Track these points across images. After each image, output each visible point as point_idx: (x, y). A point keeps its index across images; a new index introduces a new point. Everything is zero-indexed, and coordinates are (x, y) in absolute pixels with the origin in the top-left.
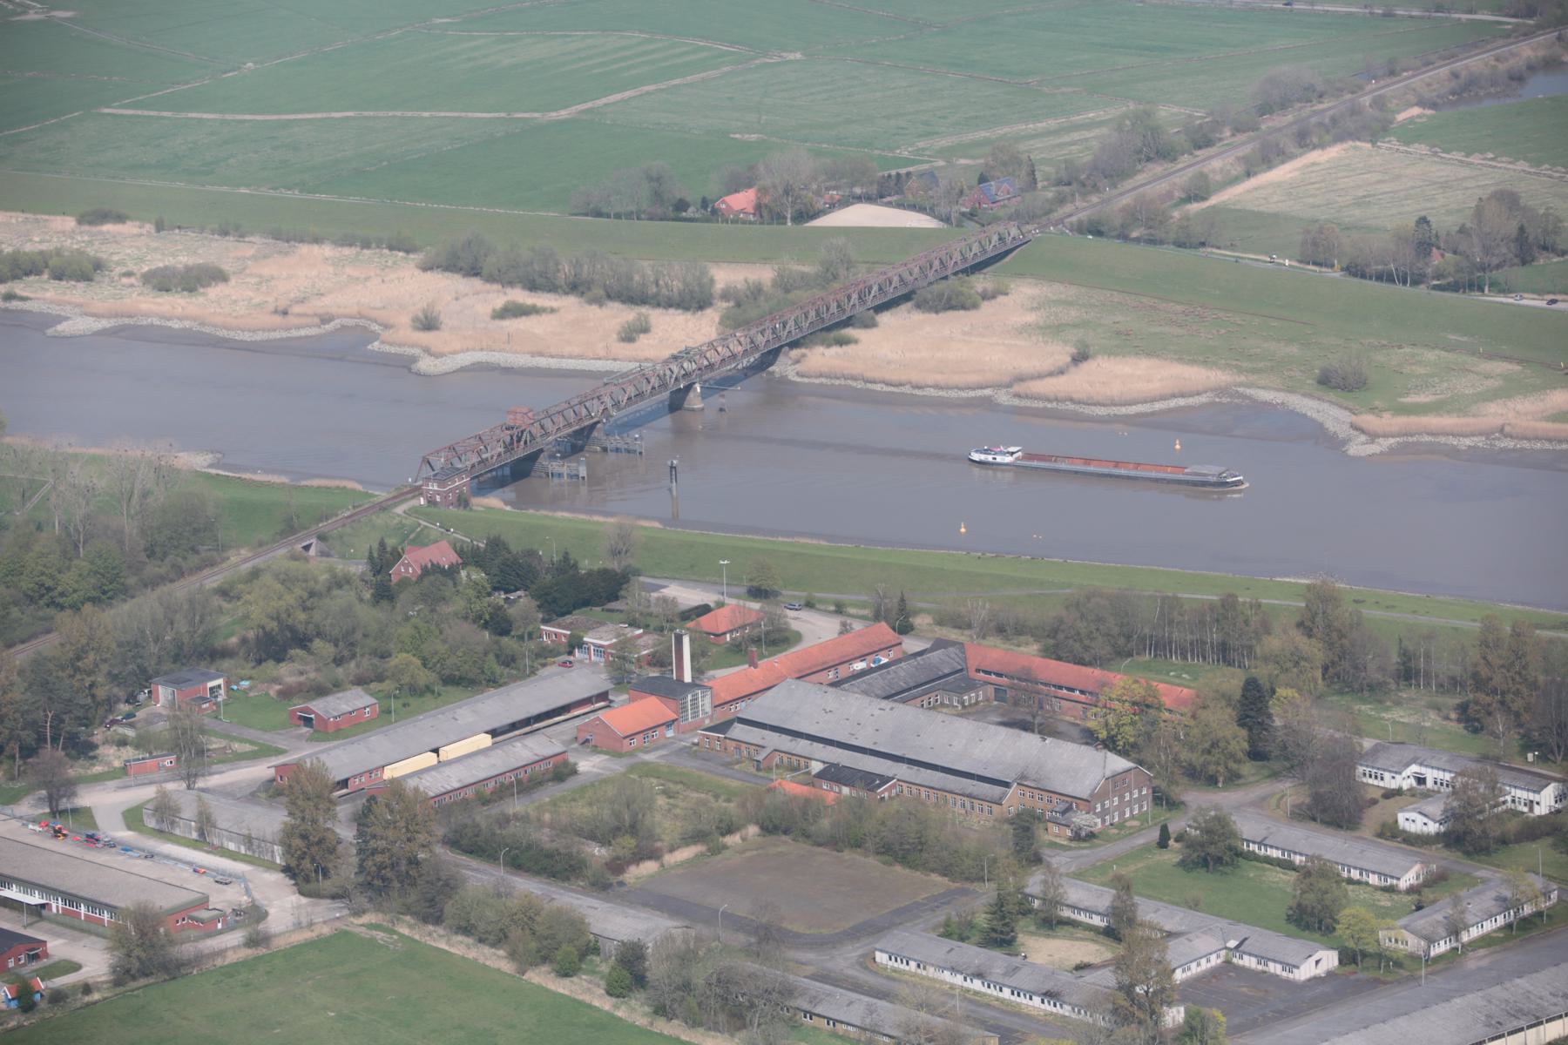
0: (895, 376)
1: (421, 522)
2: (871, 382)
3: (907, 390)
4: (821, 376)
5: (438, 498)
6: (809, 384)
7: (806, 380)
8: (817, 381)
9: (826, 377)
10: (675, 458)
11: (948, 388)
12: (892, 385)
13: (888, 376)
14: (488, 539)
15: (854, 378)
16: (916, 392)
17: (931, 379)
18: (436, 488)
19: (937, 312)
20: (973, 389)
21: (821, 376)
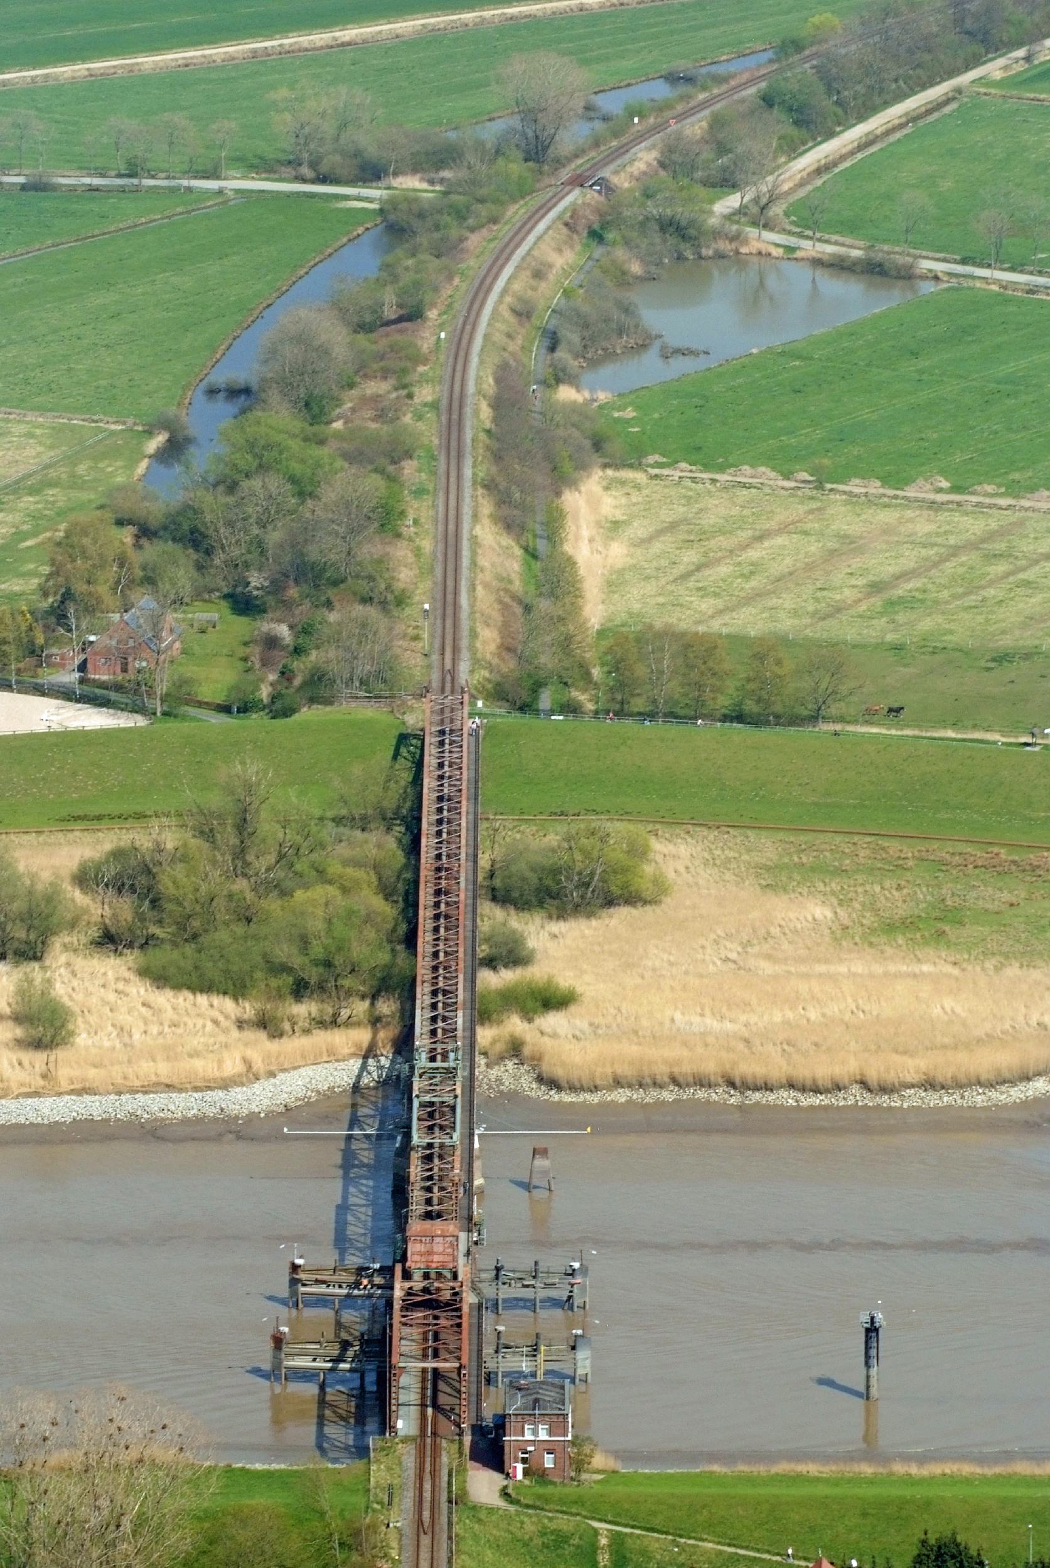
0: (823, 1070)
1: (596, 1524)
2: (756, 1088)
3: (855, 1096)
4: (618, 1083)
5: (548, 1461)
6: (602, 1105)
7: (594, 1098)
8: (621, 1096)
9: (630, 1086)
10: (877, 1307)
11: (959, 1085)
12: (817, 1091)
13: (803, 1072)
14: (924, 1543)
15: (702, 1082)
16: (884, 1100)
17: (911, 1068)
18: (543, 1435)
19: (590, 915)
20: (1012, 1082)
21: (618, 1083)
